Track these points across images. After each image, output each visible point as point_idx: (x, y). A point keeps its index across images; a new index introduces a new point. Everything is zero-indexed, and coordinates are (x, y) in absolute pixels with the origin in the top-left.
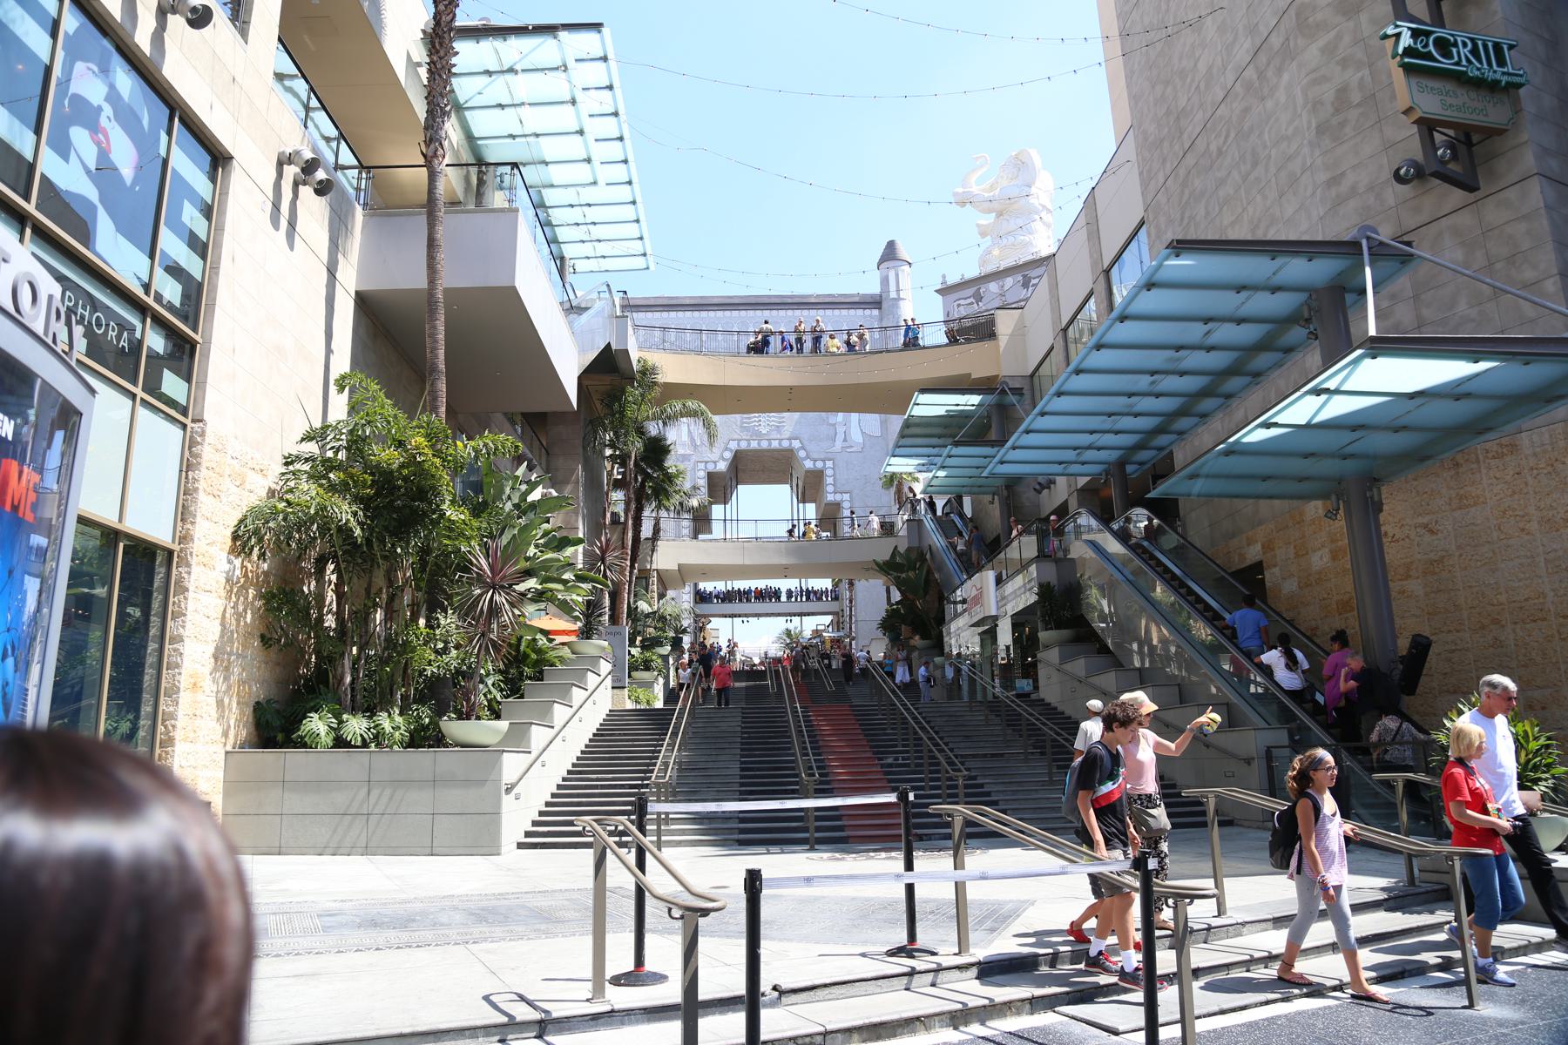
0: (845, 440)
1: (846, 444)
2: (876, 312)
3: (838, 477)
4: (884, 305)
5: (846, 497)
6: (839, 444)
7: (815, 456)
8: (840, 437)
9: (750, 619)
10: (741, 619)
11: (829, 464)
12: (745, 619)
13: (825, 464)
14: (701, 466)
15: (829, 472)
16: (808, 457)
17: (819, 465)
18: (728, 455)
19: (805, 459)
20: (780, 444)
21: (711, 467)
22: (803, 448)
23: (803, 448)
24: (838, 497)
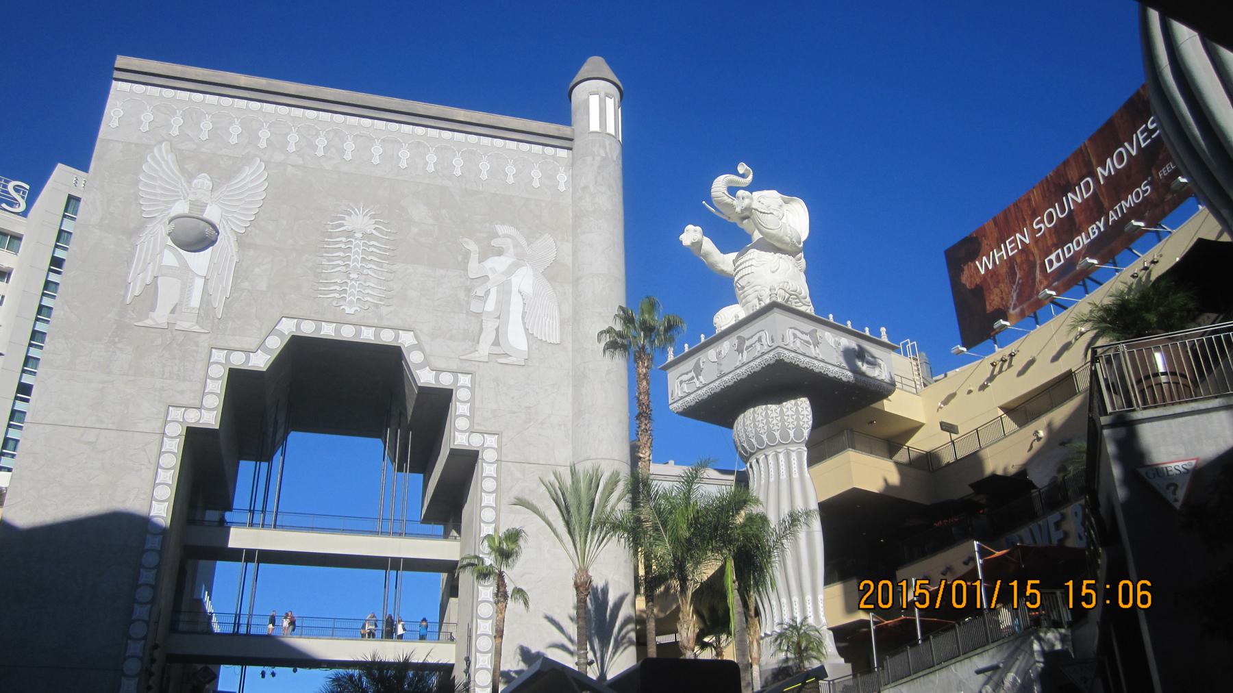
0: (496, 343)
1: (497, 350)
2: (563, 153)
3: (477, 404)
4: (577, 144)
5: (491, 441)
6: (484, 348)
7: (441, 364)
8: (488, 337)
9: (277, 669)
10: (260, 669)
11: (464, 380)
12: (268, 670)
13: (456, 380)
14: (219, 356)
15: (461, 395)
16: (426, 363)
17: (446, 381)
18: (276, 344)
19: (421, 366)
20: (377, 335)
21: (238, 361)
22: (419, 347)
23: (419, 347)
24: (474, 442)
